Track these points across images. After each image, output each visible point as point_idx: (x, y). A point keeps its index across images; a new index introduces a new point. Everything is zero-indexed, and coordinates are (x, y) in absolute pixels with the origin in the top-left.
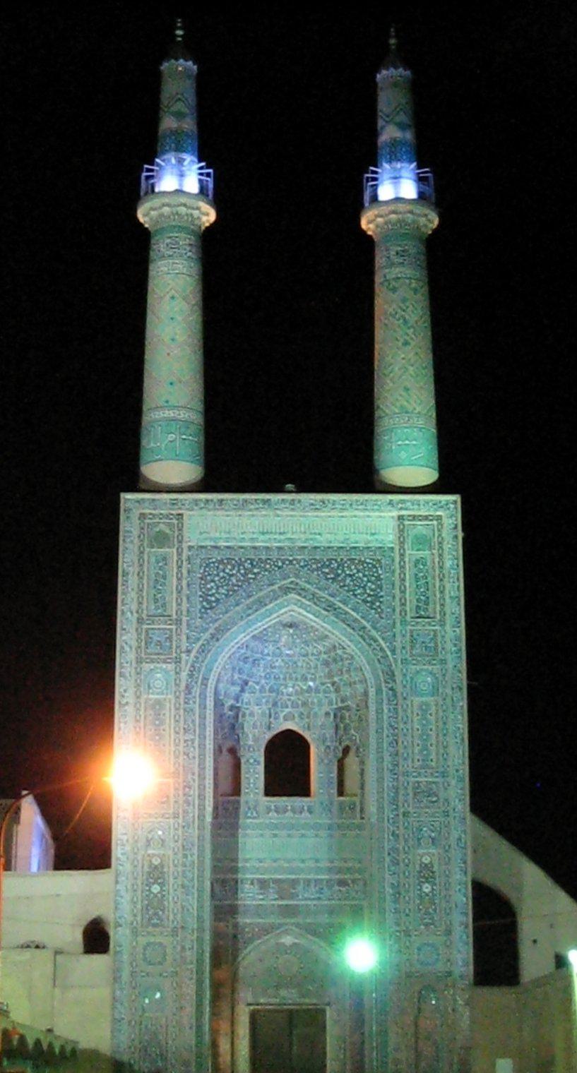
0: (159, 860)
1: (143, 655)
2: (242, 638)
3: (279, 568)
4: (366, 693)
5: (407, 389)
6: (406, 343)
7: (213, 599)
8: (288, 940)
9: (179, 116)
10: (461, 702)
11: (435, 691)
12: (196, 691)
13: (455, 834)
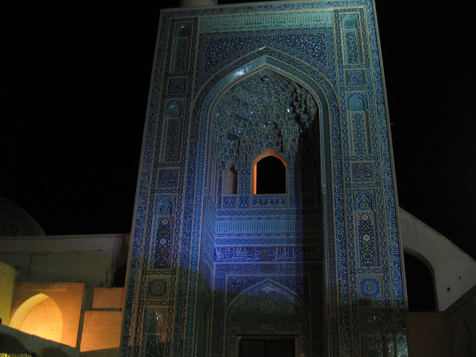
1: (167, 94)
3: (258, 41)
7: (214, 60)
8: (268, 289)
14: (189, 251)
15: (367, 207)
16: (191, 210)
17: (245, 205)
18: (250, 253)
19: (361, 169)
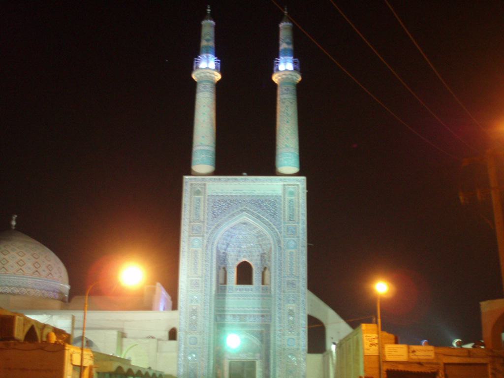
2: (227, 228)
4: (271, 249)
5: (287, 139)
6: (287, 122)
9: (208, 40)
10: (304, 251)
11: (295, 247)
12: (210, 247)
13: (301, 299)
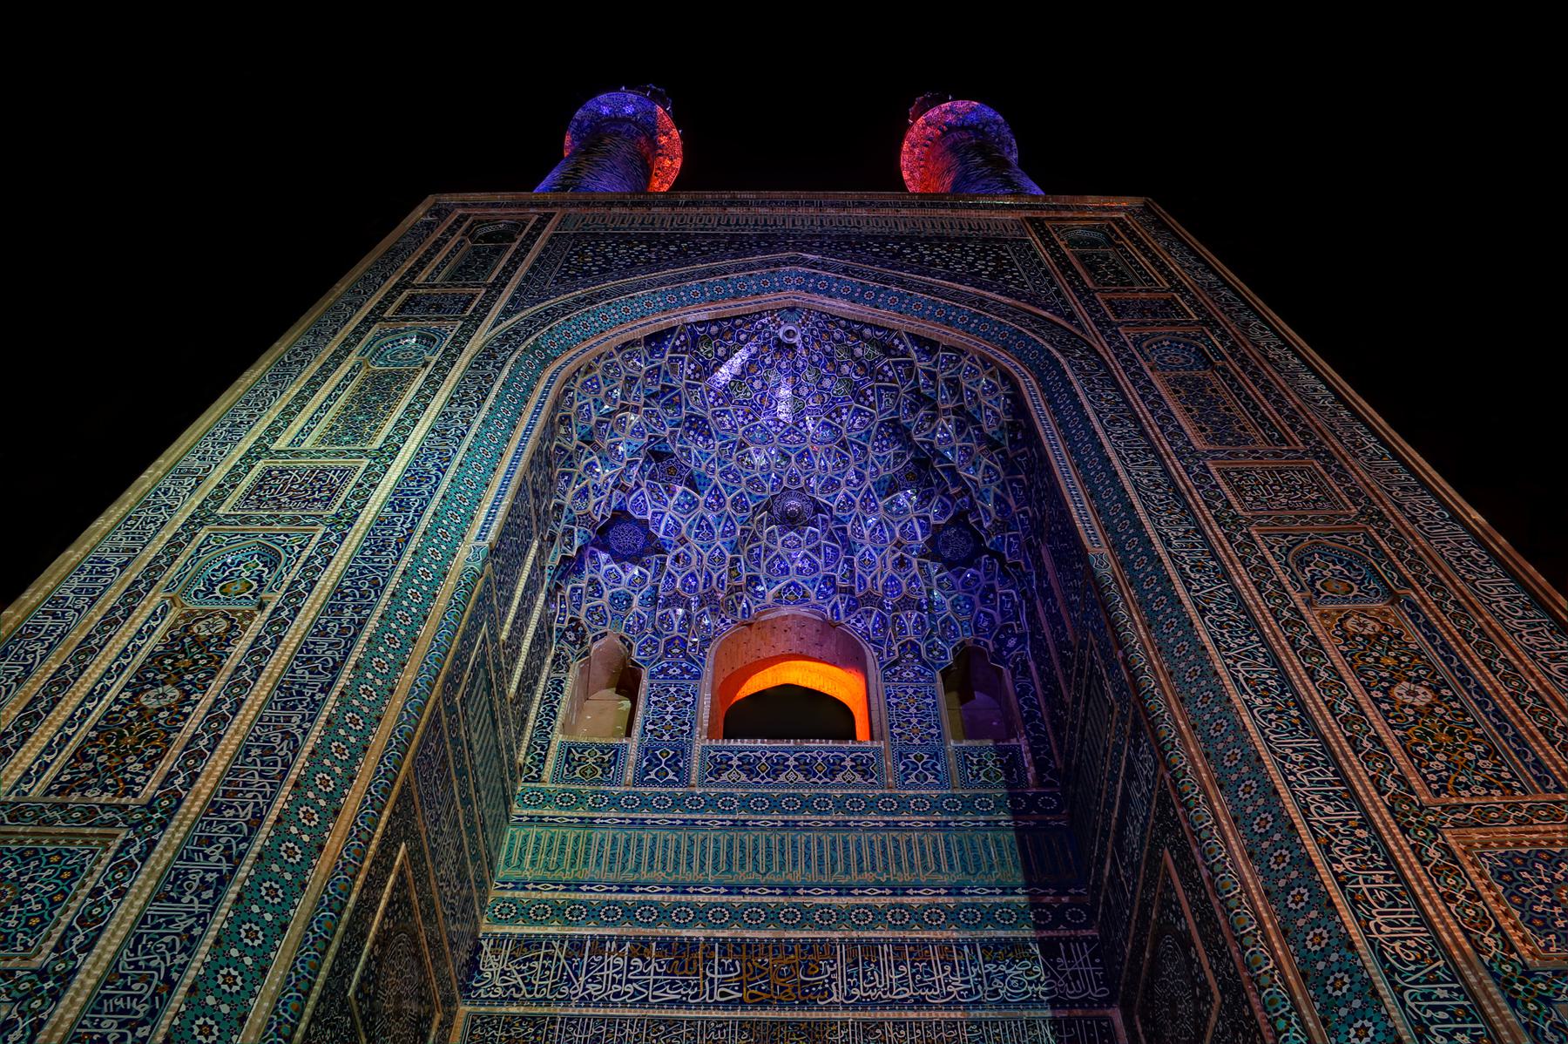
0: (224, 624)
14: (305, 732)
15: (1355, 592)
16: (374, 584)
17: (670, 776)
18: (682, 968)
19: (1266, 483)
